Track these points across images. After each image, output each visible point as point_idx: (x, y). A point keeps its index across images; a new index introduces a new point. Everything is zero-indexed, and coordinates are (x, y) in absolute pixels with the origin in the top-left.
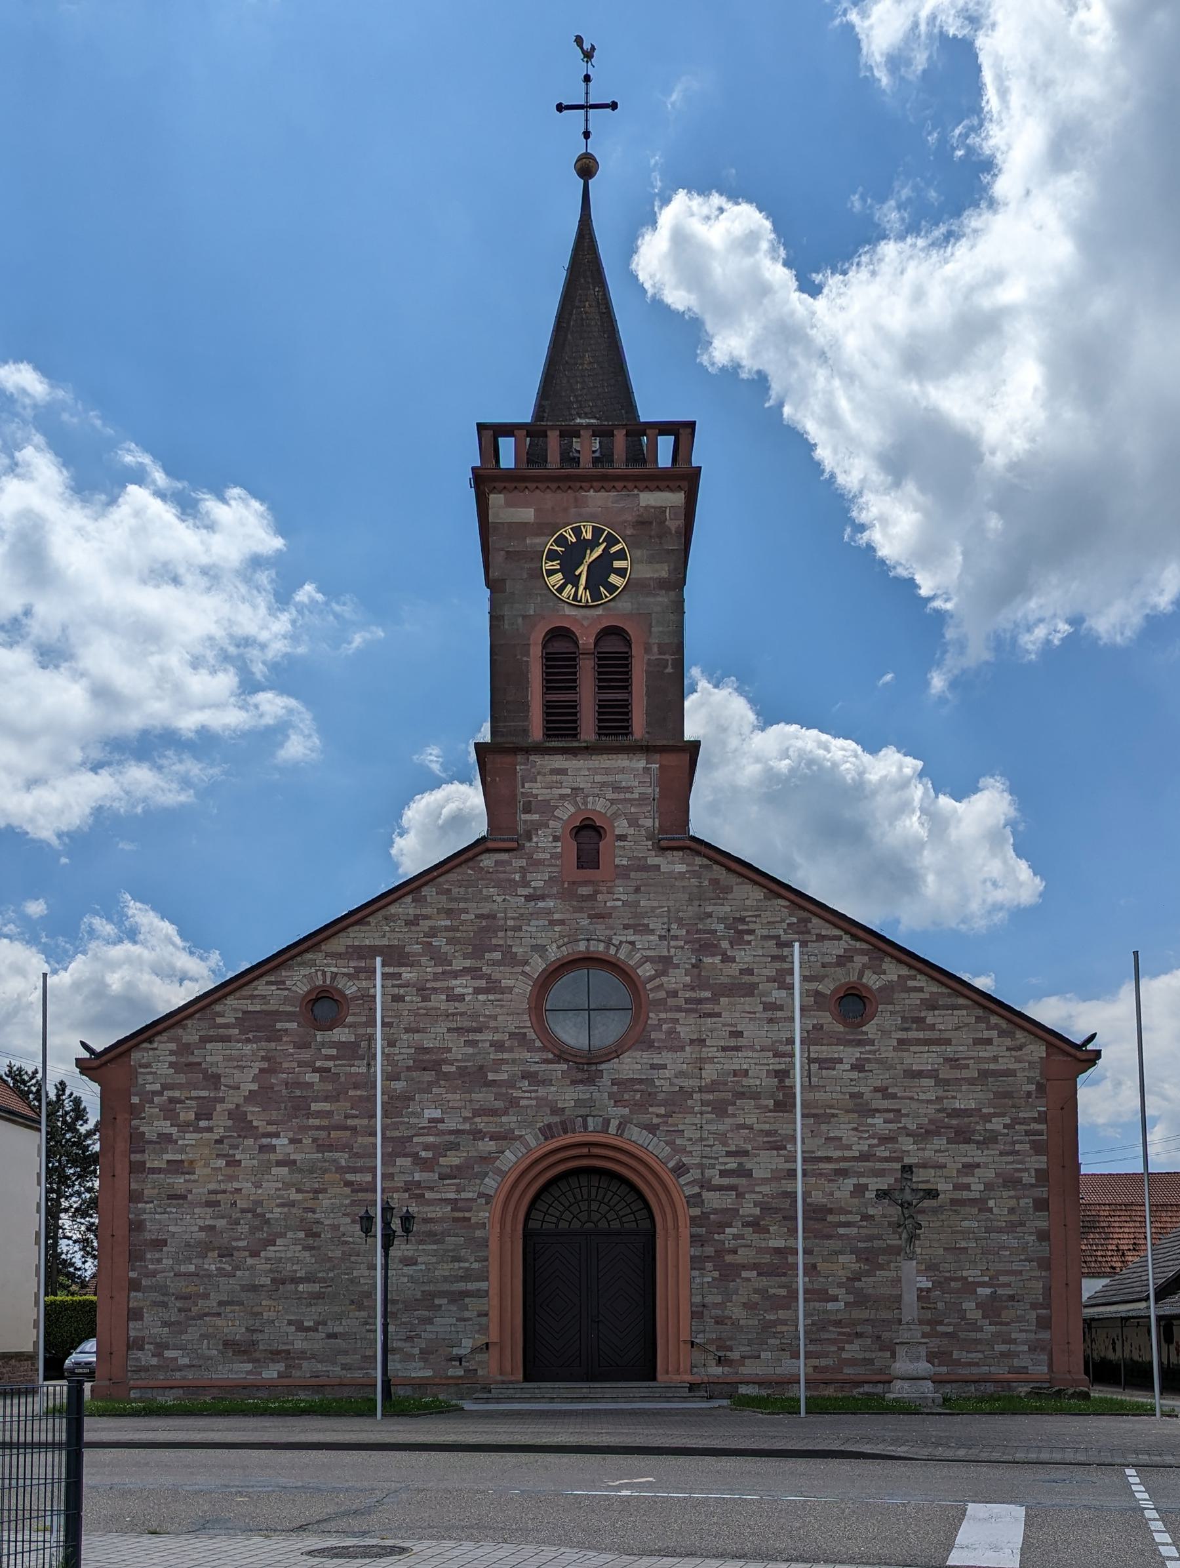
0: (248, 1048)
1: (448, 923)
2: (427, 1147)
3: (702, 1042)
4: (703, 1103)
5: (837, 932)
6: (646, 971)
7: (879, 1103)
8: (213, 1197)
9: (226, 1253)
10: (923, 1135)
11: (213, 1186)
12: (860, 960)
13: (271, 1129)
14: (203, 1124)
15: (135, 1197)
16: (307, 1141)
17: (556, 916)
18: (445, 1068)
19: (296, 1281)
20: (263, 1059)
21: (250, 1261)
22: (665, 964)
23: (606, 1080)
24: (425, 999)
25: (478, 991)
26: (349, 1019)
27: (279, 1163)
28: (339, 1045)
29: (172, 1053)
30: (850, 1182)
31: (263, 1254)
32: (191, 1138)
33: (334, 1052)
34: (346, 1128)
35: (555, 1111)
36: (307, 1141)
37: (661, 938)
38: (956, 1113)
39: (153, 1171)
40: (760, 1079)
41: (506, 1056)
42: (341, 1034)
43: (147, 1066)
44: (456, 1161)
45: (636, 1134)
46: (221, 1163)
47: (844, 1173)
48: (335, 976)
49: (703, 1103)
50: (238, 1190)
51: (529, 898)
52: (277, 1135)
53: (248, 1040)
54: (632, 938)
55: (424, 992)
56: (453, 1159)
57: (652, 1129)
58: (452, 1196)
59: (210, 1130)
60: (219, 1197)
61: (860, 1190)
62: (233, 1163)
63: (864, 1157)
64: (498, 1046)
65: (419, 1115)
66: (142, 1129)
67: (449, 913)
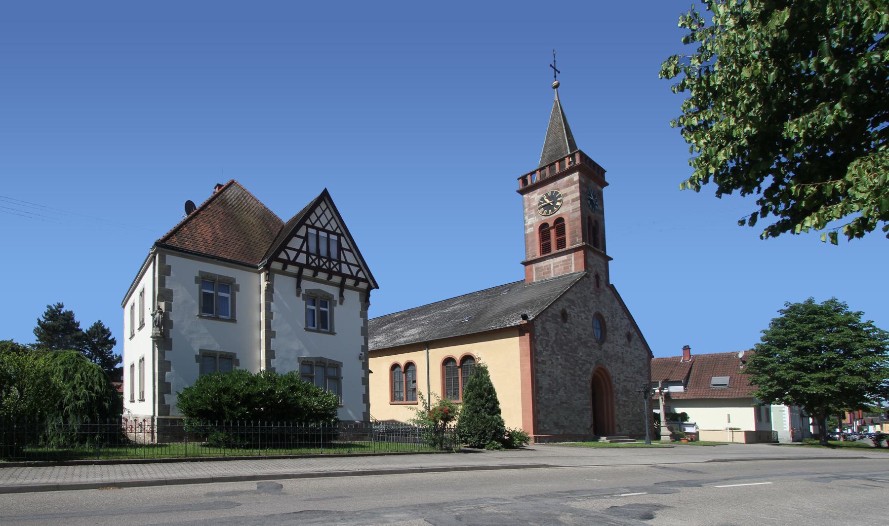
0: (553, 325)
1: (580, 296)
2: (581, 364)
3: (613, 342)
4: (615, 359)
5: (627, 317)
6: (606, 320)
7: (633, 364)
8: (550, 374)
9: (553, 392)
10: (637, 372)
11: (550, 370)
12: (629, 325)
13: (558, 353)
14: (547, 348)
15: (537, 371)
16: (563, 358)
17: (595, 300)
18: (582, 341)
19: (564, 403)
20: (556, 330)
21: (557, 396)
22: (608, 317)
23: (603, 350)
24: (578, 318)
25: (585, 318)
26: (568, 321)
27: (561, 364)
28: (567, 328)
29: (541, 323)
30: (631, 383)
31: (559, 394)
32: (545, 353)
33: (566, 330)
34: (569, 355)
35: (597, 357)
36: (563, 358)
37: (608, 311)
38: (640, 368)
39: (540, 363)
40: (620, 355)
41: (590, 339)
42: (567, 325)
43: (537, 326)
44: (585, 369)
45: (607, 366)
46: (550, 362)
47: (630, 381)
48: (566, 306)
49: (615, 359)
50: (553, 372)
51: (591, 293)
52: (558, 355)
53: (553, 323)
54: (604, 310)
55: (578, 316)
56: (584, 369)
57: (609, 365)
58: (584, 379)
59: (547, 351)
60: (550, 374)
61: (632, 385)
62: (552, 363)
63: (632, 377)
64: (588, 335)
65: (579, 354)
66: (537, 348)
67: (581, 293)
